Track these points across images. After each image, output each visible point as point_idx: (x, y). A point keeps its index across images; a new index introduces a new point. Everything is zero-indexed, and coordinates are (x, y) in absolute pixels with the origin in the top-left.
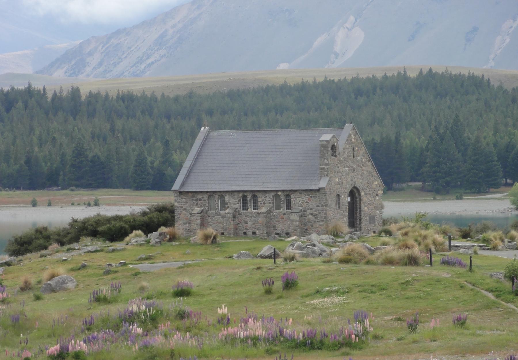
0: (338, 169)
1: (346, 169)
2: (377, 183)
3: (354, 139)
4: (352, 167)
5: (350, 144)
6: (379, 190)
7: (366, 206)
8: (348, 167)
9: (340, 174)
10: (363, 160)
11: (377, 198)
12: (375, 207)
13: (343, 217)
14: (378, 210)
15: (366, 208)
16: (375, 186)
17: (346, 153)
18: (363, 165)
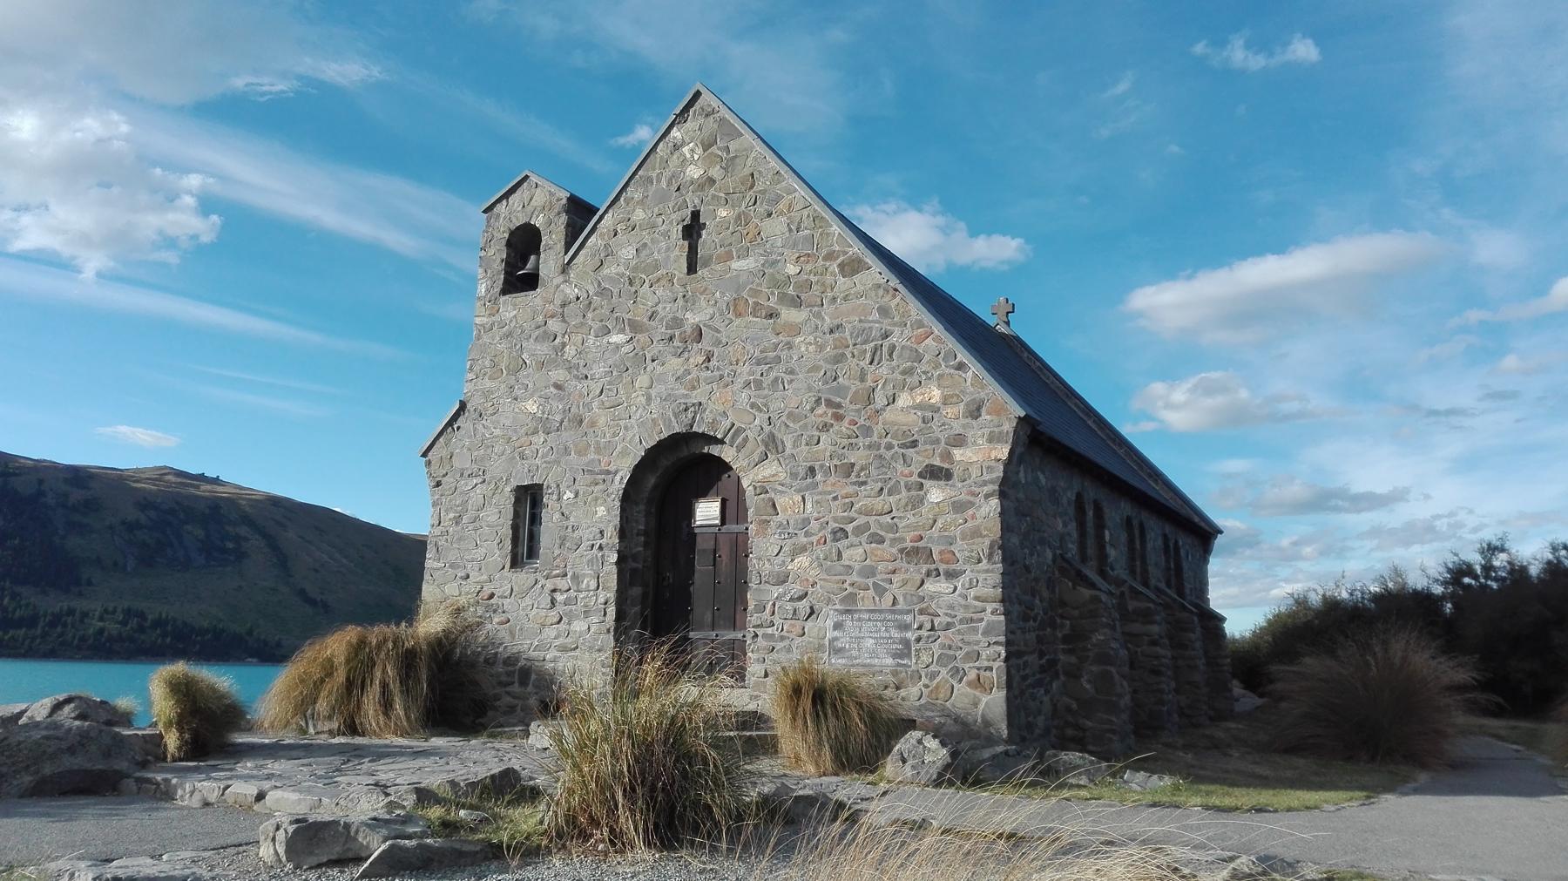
0: (543, 349)
1: (617, 338)
2: (936, 395)
3: (709, 160)
4: (677, 322)
5: (662, 198)
6: (959, 441)
7: (803, 549)
8: (635, 327)
9: (558, 375)
10: (792, 269)
11: (936, 494)
12: (915, 553)
13: (572, 617)
14: (951, 575)
15: (803, 560)
16: (913, 419)
17: (628, 253)
18: (797, 303)
